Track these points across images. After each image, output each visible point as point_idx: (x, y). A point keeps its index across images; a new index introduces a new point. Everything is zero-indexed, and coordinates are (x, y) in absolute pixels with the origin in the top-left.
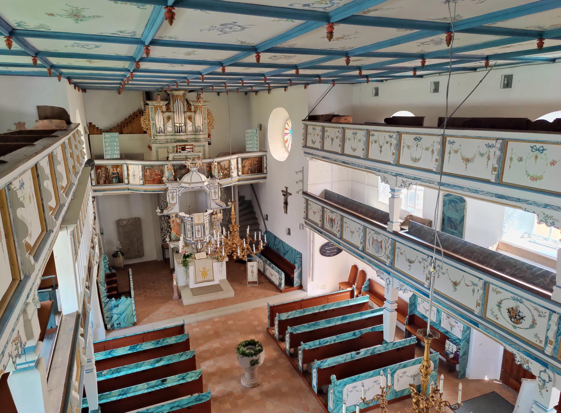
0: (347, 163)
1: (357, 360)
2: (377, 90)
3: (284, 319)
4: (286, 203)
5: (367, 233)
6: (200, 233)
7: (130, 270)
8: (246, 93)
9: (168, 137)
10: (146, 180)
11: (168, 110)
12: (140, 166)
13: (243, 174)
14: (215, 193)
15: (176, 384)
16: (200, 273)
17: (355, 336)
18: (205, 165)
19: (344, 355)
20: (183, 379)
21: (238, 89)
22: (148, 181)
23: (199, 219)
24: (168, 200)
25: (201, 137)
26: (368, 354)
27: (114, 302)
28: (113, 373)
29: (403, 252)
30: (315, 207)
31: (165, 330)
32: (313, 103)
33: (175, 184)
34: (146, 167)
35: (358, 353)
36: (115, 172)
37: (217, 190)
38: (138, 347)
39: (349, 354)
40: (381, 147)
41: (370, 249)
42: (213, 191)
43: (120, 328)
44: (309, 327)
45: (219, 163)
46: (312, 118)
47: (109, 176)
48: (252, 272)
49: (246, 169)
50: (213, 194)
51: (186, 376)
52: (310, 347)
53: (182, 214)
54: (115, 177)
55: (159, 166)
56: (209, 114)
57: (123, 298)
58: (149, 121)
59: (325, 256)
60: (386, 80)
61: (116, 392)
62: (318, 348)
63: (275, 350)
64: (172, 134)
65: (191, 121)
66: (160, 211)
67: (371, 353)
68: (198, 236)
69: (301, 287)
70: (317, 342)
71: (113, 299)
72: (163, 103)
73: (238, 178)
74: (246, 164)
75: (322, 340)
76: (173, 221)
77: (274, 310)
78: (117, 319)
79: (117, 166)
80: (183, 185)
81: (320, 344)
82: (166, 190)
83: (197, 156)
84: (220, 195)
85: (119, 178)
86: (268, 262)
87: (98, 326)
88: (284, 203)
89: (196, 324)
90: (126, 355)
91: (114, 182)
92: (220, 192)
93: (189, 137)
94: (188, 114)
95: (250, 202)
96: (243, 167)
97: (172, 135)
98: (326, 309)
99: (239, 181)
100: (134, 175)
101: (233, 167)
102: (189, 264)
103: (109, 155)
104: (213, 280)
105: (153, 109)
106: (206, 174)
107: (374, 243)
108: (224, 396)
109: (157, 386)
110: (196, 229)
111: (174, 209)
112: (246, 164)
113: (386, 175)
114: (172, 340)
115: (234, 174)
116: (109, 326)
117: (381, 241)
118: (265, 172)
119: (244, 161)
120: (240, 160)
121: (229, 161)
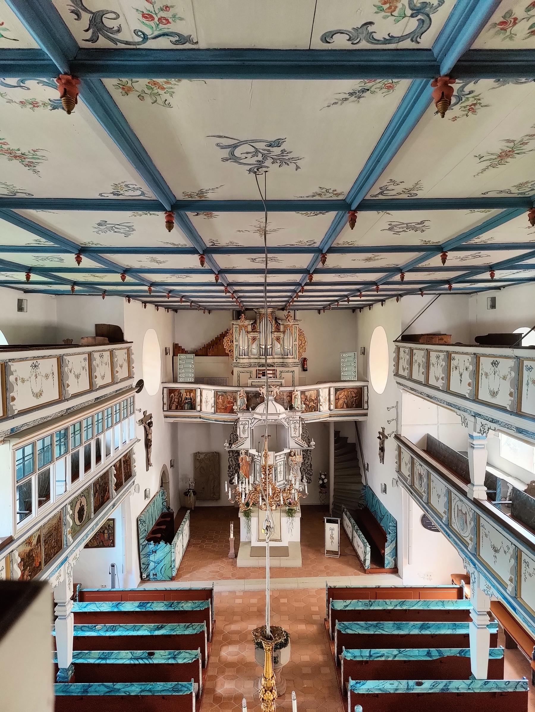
0: (431, 398)
1: (418, 694)
2: (493, 300)
3: (339, 609)
4: (382, 449)
5: (453, 499)
7: (189, 511)
8: (354, 309)
9: (252, 361)
10: (218, 408)
11: (254, 330)
14: (295, 428)
15: (163, 662)
16: (271, 530)
17: (430, 656)
18: (285, 394)
19: (396, 683)
20: (174, 658)
21: (329, 305)
24: (238, 433)
25: (290, 361)
26: (436, 690)
27: (152, 546)
28: (107, 631)
29: (487, 533)
30: (406, 455)
31: (190, 591)
32: (408, 321)
33: (247, 415)
34: (219, 393)
35: (419, 684)
36: (187, 397)
37: (297, 425)
38: (149, 605)
39: (404, 682)
40: (461, 375)
41: (456, 525)
42: (292, 426)
43: (156, 580)
44: (366, 629)
45: (303, 393)
46: (407, 338)
48: (332, 538)
49: (341, 402)
51: (178, 654)
52: (355, 657)
53: (253, 452)
55: (233, 392)
56: (301, 334)
57: (162, 543)
58: (232, 342)
59: (430, 529)
60: (504, 287)
61: (96, 653)
62: (367, 662)
63: (323, 654)
64: (256, 357)
65: (279, 343)
66: (228, 445)
67: (442, 689)
69: (395, 570)
70: (366, 652)
71: (152, 542)
72: (247, 322)
73: (329, 412)
74: (340, 396)
75: (373, 651)
76: (242, 459)
77: (334, 593)
78: (154, 568)
79: (190, 391)
80: (256, 416)
81: (370, 656)
82: (237, 420)
83: (279, 383)
84: (301, 432)
85: (191, 404)
86: (356, 526)
87: (129, 572)
88: (380, 449)
89: (242, 594)
90: (133, 612)
91: (186, 408)
92: (301, 428)
93: (275, 360)
94: (276, 334)
95: (354, 445)
96: (337, 399)
97: (256, 358)
98: (405, 608)
100: (207, 402)
101: (322, 400)
102: (252, 514)
103: (183, 377)
104: (280, 540)
105: (238, 329)
106: (285, 404)
107: (459, 515)
108: (230, 698)
109: (142, 659)
111: (245, 445)
113: (465, 414)
114: (187, 606)
115: (324, 407)
116: (144, 576)
117: (466, 514)
118: (366, 407)
119: (338, 392)
120: (332, 391)
121: (318, 391)
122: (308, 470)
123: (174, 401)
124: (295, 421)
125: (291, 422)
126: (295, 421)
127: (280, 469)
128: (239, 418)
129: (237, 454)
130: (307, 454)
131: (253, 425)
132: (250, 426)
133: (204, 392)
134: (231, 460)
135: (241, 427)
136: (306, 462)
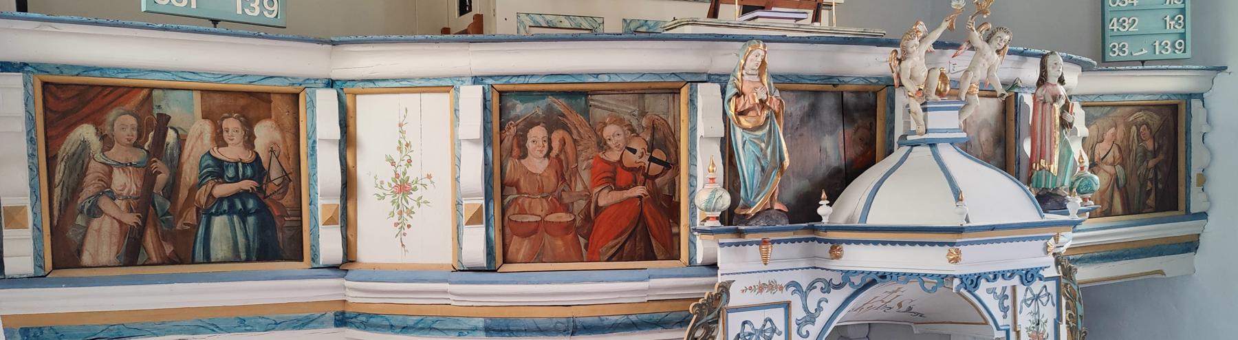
12: (472, 98)
22: (530, 231)
33: (788, 259)
34: (520, 109)
37: (1048, 312)
54: (229, 206)
80: (862, 258)
91: (219, 248)
100: (403, 188)
123: (106, 190)
128: (725, 288)
133: (372, 114)
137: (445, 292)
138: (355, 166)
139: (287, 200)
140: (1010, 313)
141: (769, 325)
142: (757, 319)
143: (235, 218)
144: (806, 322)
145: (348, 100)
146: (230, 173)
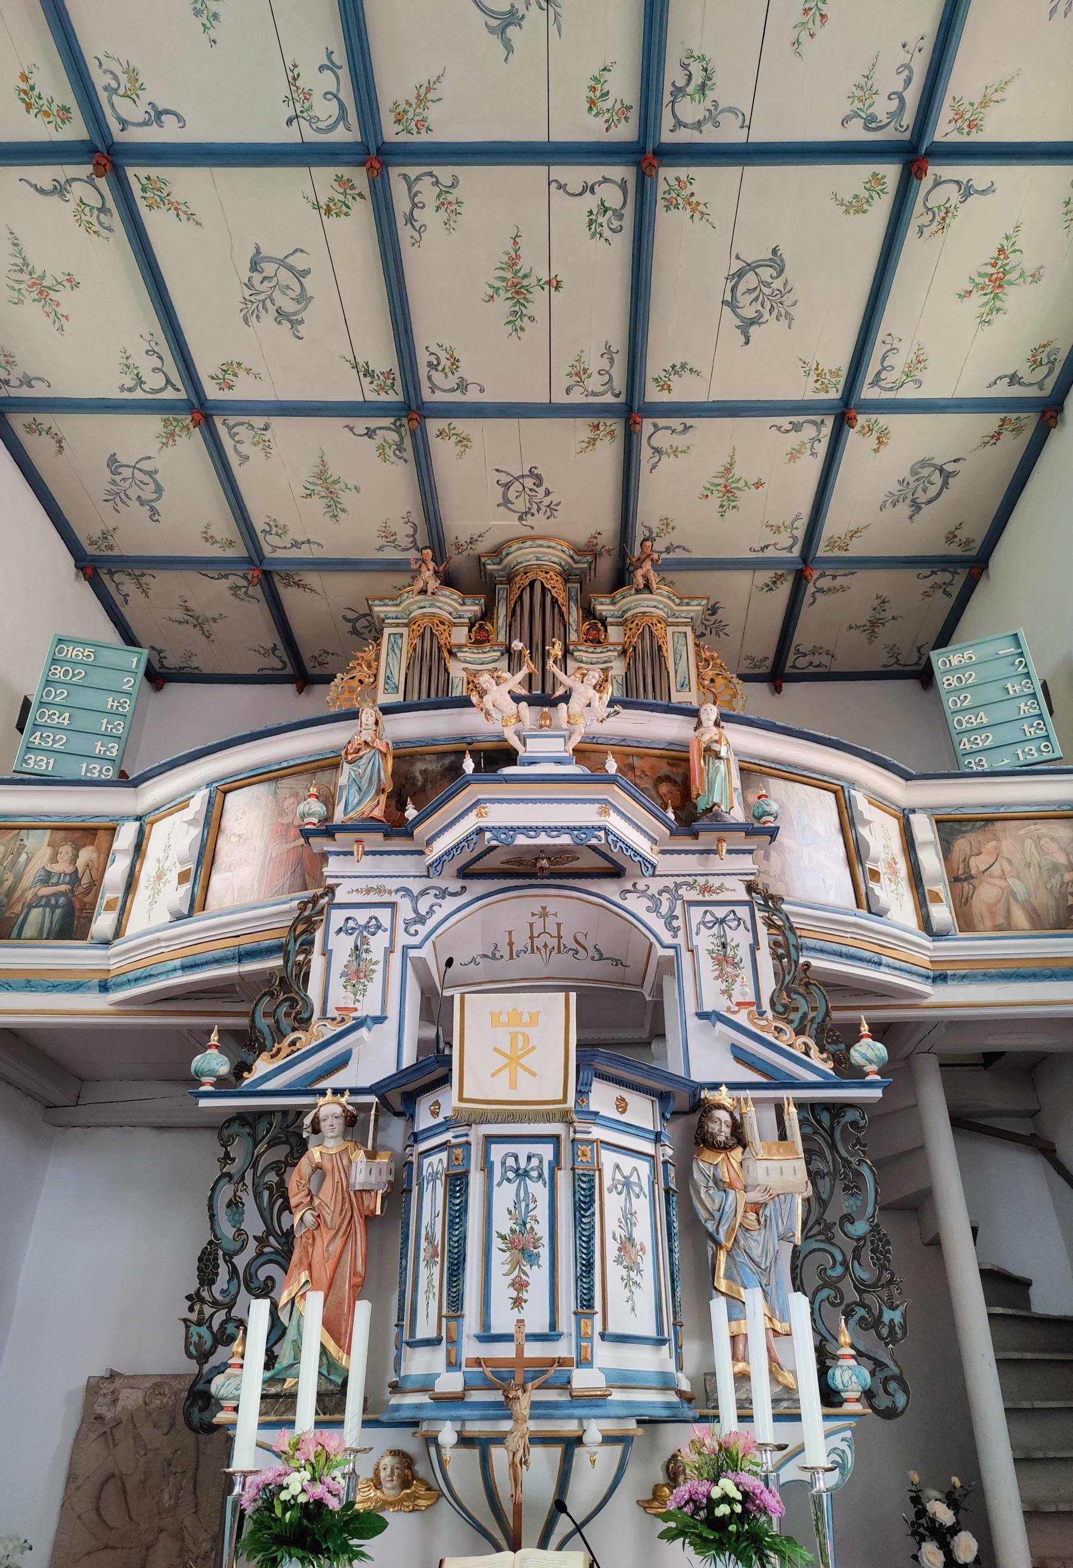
6: (538, 1277)
13: (966, 921)
14: (723, 956)
23: (513, 1061)
24: (314, 991)
36: (56, 868)
37: (740, 938)
42: (705, 941)
47: (12, 890)
50: (707, 964)
68: (516, 1304)
84: (769, 985)
91: (29, 930)
92: (765, 956)
96: (960, 879)
99: (940, 978)
110: (502, 1224)
112: (977, 864)
119: (961, 845)
120: (924, 829)
122: (861, 1287)
124: (720, 912)
125: (696, 913)
126: (720, 912)
127: (628, 1217)
128: (331, 890)
129: (280, 1153)
130: (833, 1147)
131: (423, 930)
132: (402, 939)
134: (235, 1204)
135: (342, 946)
136: (832, 1216)
137: (158, 940)
138: (140, 872)
139: (88, 899)
140: (681, 934)
141: (373, 922)
142: (362, 916)
143: (48, 909)
144: (415, 923)
145: (147, 829)
146: (54, 880)
